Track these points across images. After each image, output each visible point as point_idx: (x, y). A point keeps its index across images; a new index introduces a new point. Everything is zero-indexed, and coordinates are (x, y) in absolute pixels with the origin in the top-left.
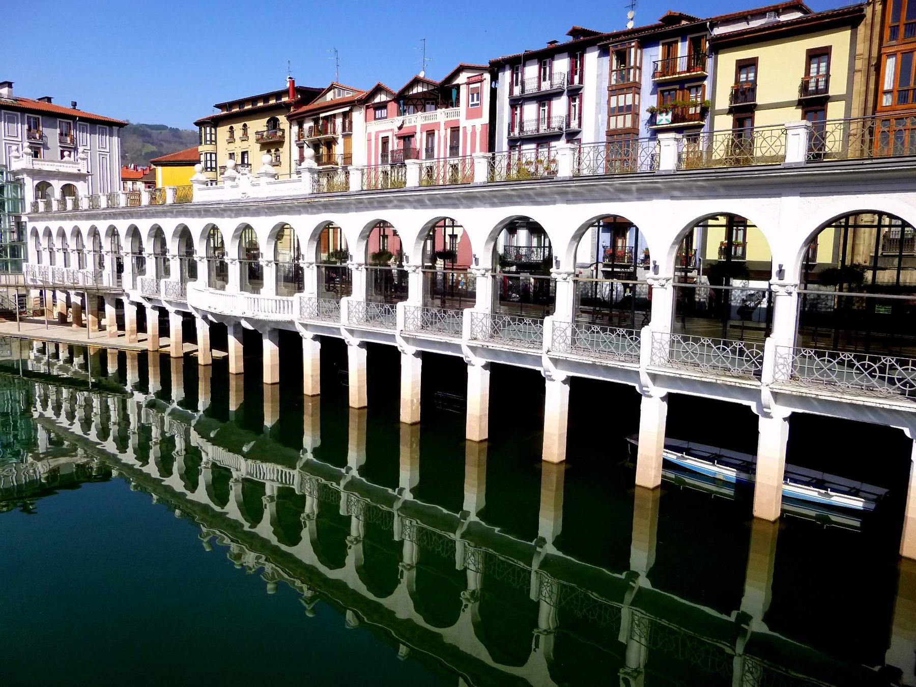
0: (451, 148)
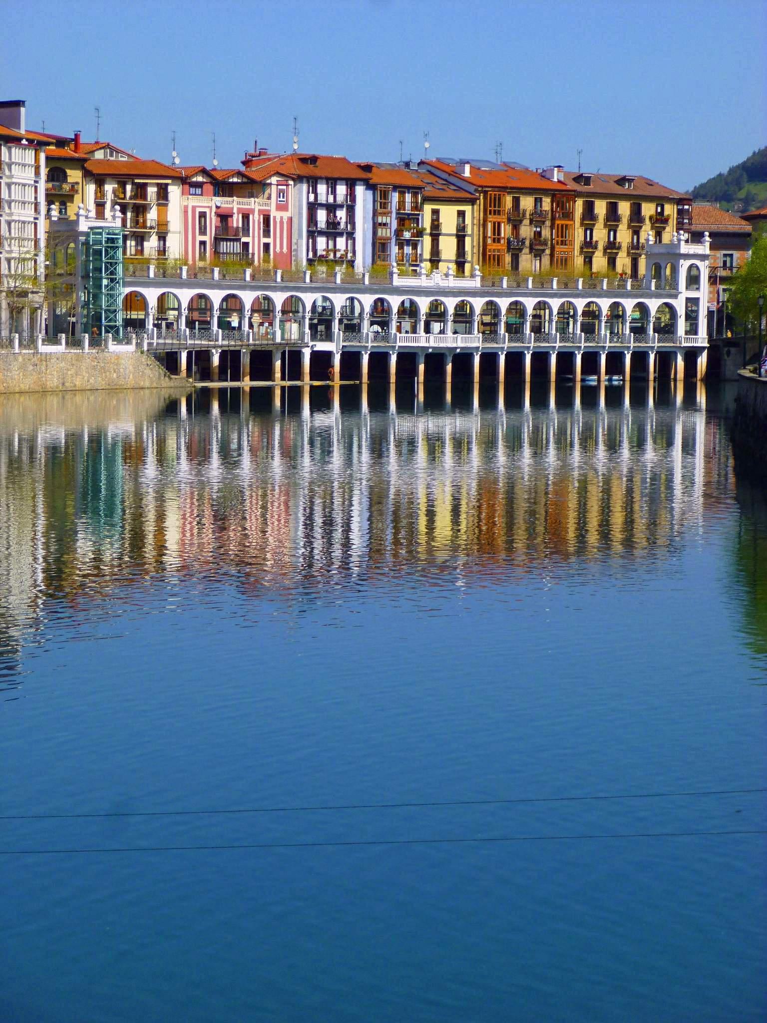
0: (264, 231)
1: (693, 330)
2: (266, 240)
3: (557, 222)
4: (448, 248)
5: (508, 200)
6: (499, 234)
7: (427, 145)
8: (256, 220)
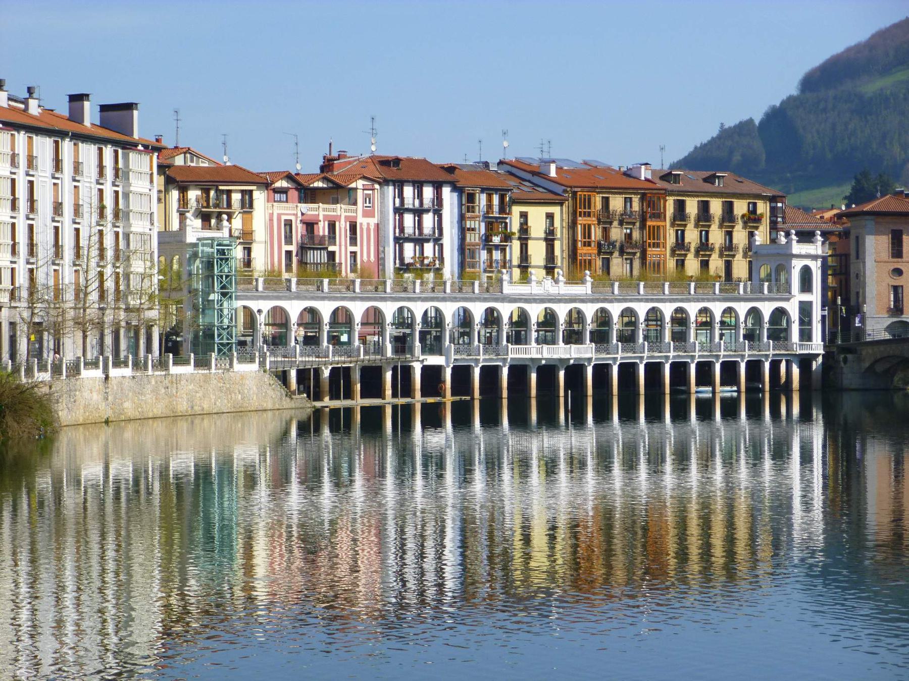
0: (351, 238)
1: (806, 335)
2: (353, 249)
3: (649, 223)
4: (537, 252)
5: (598, 201)
6: (590, 237)
7: (506, 144)
8: (342, 227)
